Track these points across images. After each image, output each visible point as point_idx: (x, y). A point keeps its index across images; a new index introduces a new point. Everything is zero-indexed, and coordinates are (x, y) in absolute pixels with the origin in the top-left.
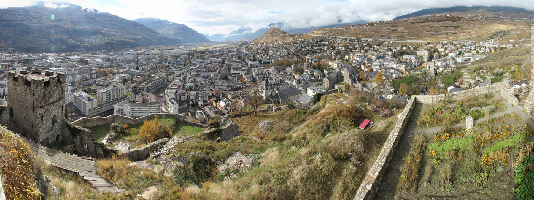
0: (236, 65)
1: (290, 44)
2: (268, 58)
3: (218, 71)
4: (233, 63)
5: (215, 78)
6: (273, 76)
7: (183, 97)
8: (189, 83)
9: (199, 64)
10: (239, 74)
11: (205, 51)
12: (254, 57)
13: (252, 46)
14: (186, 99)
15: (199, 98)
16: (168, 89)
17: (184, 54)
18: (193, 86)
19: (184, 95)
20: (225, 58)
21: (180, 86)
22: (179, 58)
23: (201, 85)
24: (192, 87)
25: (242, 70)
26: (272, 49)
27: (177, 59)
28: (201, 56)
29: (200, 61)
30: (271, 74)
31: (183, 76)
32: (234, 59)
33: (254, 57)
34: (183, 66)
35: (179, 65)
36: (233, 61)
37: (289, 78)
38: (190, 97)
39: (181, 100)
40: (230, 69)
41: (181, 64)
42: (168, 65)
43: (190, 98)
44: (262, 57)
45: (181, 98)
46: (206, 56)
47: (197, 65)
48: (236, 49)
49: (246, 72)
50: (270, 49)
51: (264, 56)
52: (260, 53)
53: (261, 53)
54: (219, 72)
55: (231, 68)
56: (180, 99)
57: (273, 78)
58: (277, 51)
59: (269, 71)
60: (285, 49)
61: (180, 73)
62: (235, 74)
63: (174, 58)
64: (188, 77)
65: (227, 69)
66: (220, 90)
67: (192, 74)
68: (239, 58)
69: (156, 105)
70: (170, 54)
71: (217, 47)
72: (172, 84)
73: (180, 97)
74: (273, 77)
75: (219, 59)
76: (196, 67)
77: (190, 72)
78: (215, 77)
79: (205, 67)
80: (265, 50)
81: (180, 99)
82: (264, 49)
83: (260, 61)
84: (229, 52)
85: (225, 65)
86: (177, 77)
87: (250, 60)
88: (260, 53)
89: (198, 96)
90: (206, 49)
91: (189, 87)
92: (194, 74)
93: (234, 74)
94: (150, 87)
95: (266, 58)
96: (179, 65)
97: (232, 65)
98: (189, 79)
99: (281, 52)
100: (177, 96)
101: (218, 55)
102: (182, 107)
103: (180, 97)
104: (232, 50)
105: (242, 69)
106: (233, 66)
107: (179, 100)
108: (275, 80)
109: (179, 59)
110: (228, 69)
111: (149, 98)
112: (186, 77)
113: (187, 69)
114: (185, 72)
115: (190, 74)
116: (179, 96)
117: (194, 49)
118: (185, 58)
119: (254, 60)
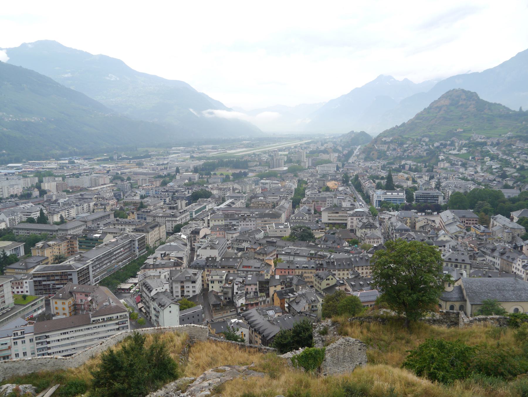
0: (335, 201)
1: (510, 145)
2: (433, 184)
3: (284, 216)
4: (328, 193)
5: (279, 234)
6: (447, 238)
7: (191, 285)
8: (205, 248)
9: (231, 197)
10: (346, 224)
11: (245, 159)
12: (389, 178)
13: (385, 148)
14: (198, 291)
15: (236, 287)
16: (145, 268)
17: (187, 171)
18: (217, 256)
19: (194, 282)
20: (305, 179)
21: (181, 258)
22: (171, 180)
23: (240, 254)
24: (214, 259)
25: (352, 215)
26: (447, 159)
27: (164, 184)
28: (233, 175)
29: (234, 190)
30: (442, 232)
31: (189, 232)
32: (331, 184)
33: (389, 178)
34: (184, 202)
35: (174, 199)
36: (328, 189)
37: (499, 250)
38: (211, 285)
39: (186, 294)
40: (318, 212)
41: (178, 198)
42: (141, 203)
43: (210, 289)
44: (414, 181)
45: (186, 290)
46: (250, 174)
47: (224, 200)
48: (336, 155)
49: (365, 220)
50: (441, 157)
51: (420, 177)
52: (407, 167)
53: (410, 169)
54: (287, 220)
55: (322, 209)
56: (183, 292)
57: (447, 245)
58: (464, 165)
59: (434, 221)
60: (492, 159)
61: (178, 223)
62: (334, 224)
63: (158, 183)
64: (202, 234)
65: (309, 210)
66: (292, 267)
67: (211, 225)
68: (345, 181)
69: (114, 316)
70: (145, 171)
71: (280, 150)
72: (158, 254)
73: (183, 287)
74: (447, 241)
75: (287, 183)
76: (222, 206)
77: (206, 219)
78: (278, 230)
79: (248, 206)
80: (424, 162)
81: (183, 292)
82: (422, 157)
83: (409, 193)
84: (315, 164)
85: (305, 199)
86: (168, 234)
87: (379, 187)
88: (407, 167)
89: (231, 281)
90: (249, 155)
91: (207, 259)
92: (217, 223)
93: (328, 224)
94: (91, 269)
95: (428, 183)
96: (174, 199)
97: (324, 200)
98: (204, 237)
99: (479, 169)
100: (174, 285)
101: (284, 172)
102: (189, 312)
103: (183, 287)
104: (325, 157)
105: (351, 212)
106: (329, 201)
107: (179, 294)
108: (454, 248)
109: (171, 184)
110: (313, 212)
111: (89, 299)
112: (196, 232)
113: (196, 212)
114: (192, 219)
115: (206, 225)
116: (179, 285)
117: (214, 153)
118: (190, 180)
119: (390, 186)
